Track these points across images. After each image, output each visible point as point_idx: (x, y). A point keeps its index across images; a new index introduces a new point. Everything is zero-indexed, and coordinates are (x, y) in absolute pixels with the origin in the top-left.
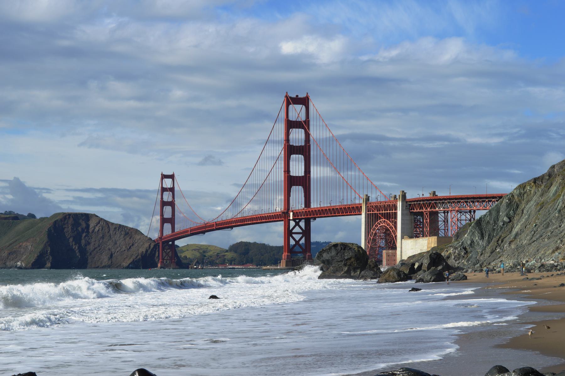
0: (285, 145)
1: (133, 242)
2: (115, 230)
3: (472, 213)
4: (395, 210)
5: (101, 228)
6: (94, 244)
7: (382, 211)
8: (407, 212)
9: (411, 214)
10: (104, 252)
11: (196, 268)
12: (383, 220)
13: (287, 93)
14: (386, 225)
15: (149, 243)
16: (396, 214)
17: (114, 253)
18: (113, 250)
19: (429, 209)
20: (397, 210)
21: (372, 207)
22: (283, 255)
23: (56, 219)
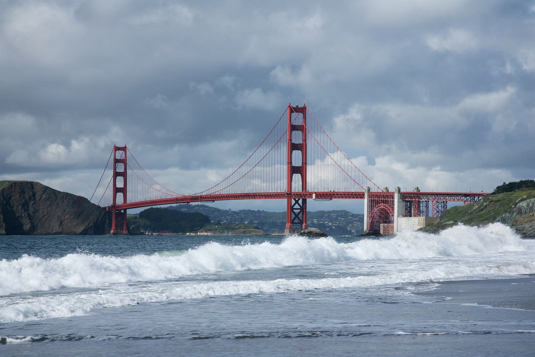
0: (288, 143)
1: (82, 209)
2: (62, 198)
3: (445, 203)
4: (392, 198)
6: (43, 212)
7: (382, 198)
8: (401, 200)
9: (403, 202)
10: (54, 220)
11: (147, 235)
12: (383, 204)
13: (290, 104)
14: (383, 207)
15: (100, 211)
16: (393, 201)
17: (64, 220)
18: (62, 218)
19: (417, 200)
20: (394, 199)
21: (373, 196)
22: (287, 225)
23: (3, 187)
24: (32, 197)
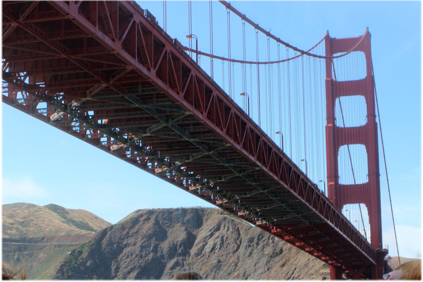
2: (250, 246)
5: (218, 240)
24: (180, 246)
